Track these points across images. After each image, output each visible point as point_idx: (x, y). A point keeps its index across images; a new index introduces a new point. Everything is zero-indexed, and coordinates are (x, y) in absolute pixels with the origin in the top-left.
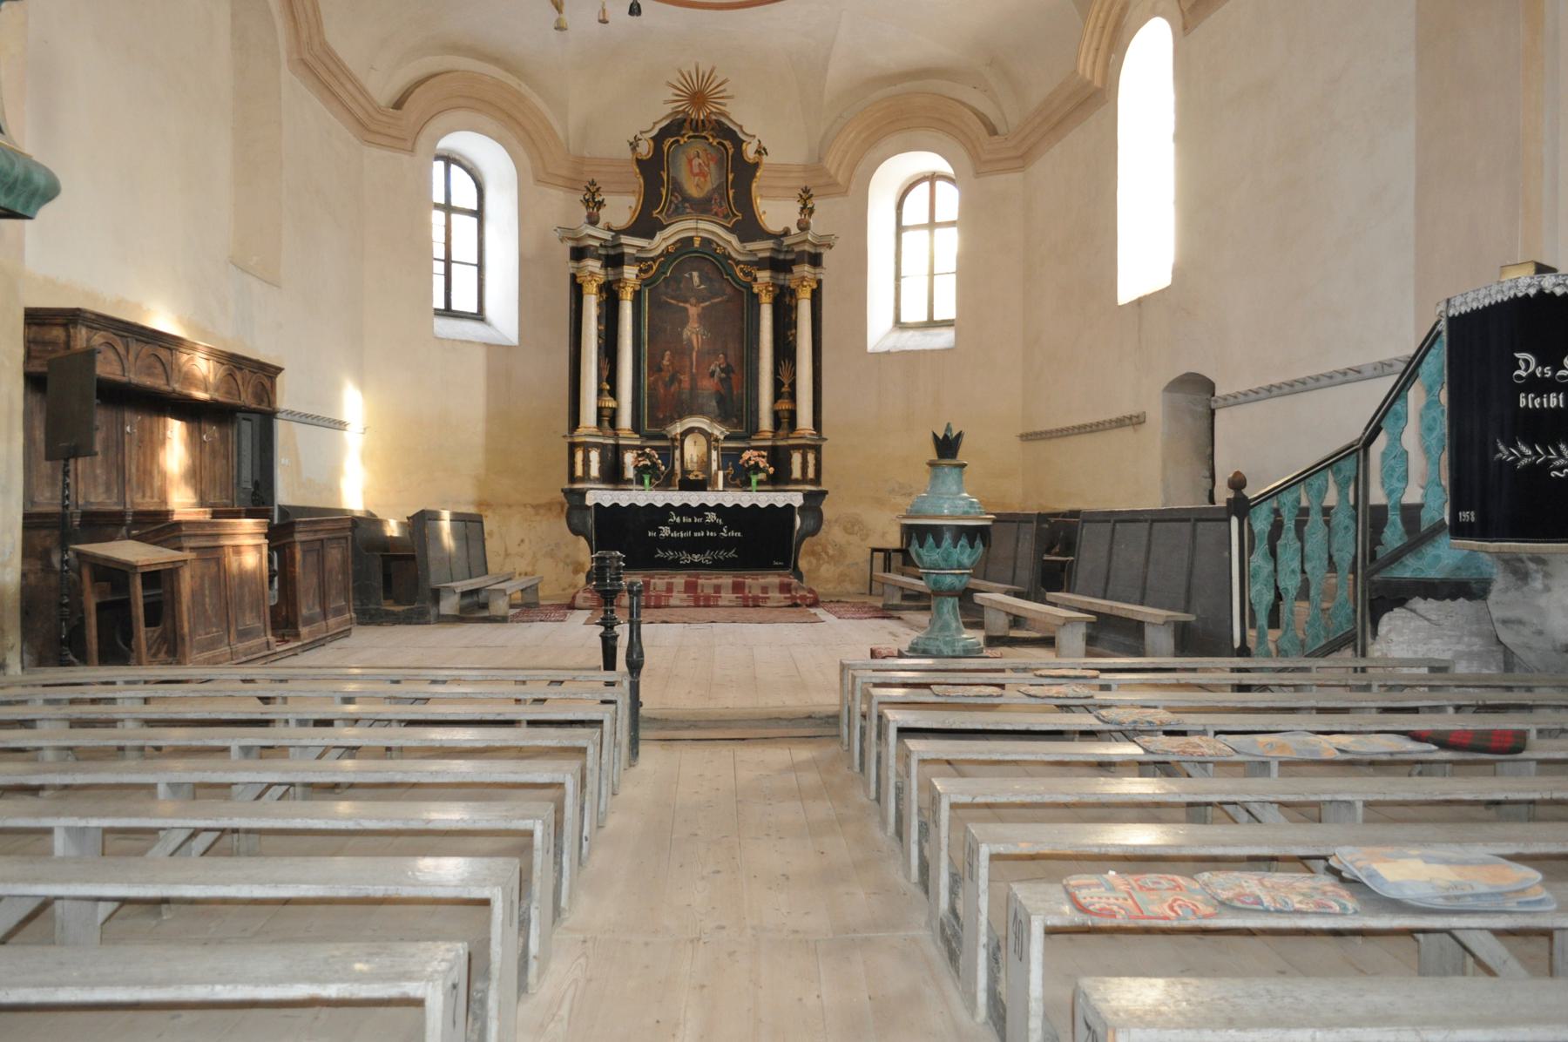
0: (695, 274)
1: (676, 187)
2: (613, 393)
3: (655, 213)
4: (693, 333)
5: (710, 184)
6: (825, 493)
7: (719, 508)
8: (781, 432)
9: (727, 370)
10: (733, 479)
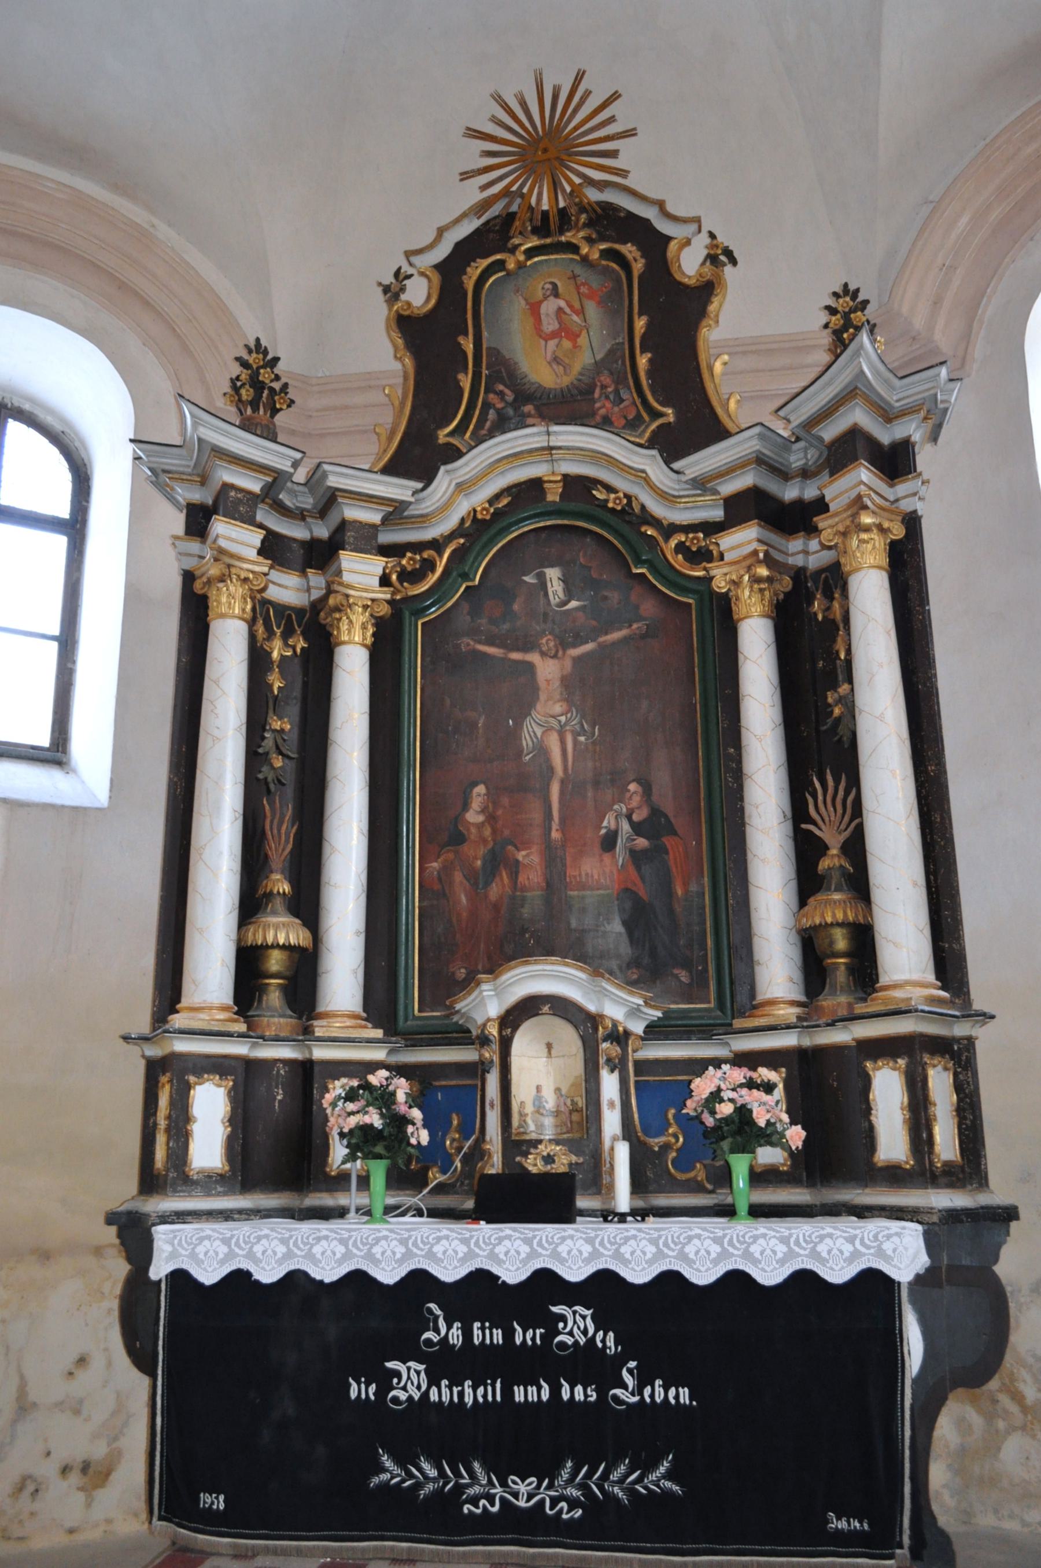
0: (553, 574)
1: (501, 371)
2: (307, 906)
3: (443, 435)
4: (550, 728)
6: (1008, 1215)
7: (603, 1289)
8: (836, 1001)
9: (654, 826)
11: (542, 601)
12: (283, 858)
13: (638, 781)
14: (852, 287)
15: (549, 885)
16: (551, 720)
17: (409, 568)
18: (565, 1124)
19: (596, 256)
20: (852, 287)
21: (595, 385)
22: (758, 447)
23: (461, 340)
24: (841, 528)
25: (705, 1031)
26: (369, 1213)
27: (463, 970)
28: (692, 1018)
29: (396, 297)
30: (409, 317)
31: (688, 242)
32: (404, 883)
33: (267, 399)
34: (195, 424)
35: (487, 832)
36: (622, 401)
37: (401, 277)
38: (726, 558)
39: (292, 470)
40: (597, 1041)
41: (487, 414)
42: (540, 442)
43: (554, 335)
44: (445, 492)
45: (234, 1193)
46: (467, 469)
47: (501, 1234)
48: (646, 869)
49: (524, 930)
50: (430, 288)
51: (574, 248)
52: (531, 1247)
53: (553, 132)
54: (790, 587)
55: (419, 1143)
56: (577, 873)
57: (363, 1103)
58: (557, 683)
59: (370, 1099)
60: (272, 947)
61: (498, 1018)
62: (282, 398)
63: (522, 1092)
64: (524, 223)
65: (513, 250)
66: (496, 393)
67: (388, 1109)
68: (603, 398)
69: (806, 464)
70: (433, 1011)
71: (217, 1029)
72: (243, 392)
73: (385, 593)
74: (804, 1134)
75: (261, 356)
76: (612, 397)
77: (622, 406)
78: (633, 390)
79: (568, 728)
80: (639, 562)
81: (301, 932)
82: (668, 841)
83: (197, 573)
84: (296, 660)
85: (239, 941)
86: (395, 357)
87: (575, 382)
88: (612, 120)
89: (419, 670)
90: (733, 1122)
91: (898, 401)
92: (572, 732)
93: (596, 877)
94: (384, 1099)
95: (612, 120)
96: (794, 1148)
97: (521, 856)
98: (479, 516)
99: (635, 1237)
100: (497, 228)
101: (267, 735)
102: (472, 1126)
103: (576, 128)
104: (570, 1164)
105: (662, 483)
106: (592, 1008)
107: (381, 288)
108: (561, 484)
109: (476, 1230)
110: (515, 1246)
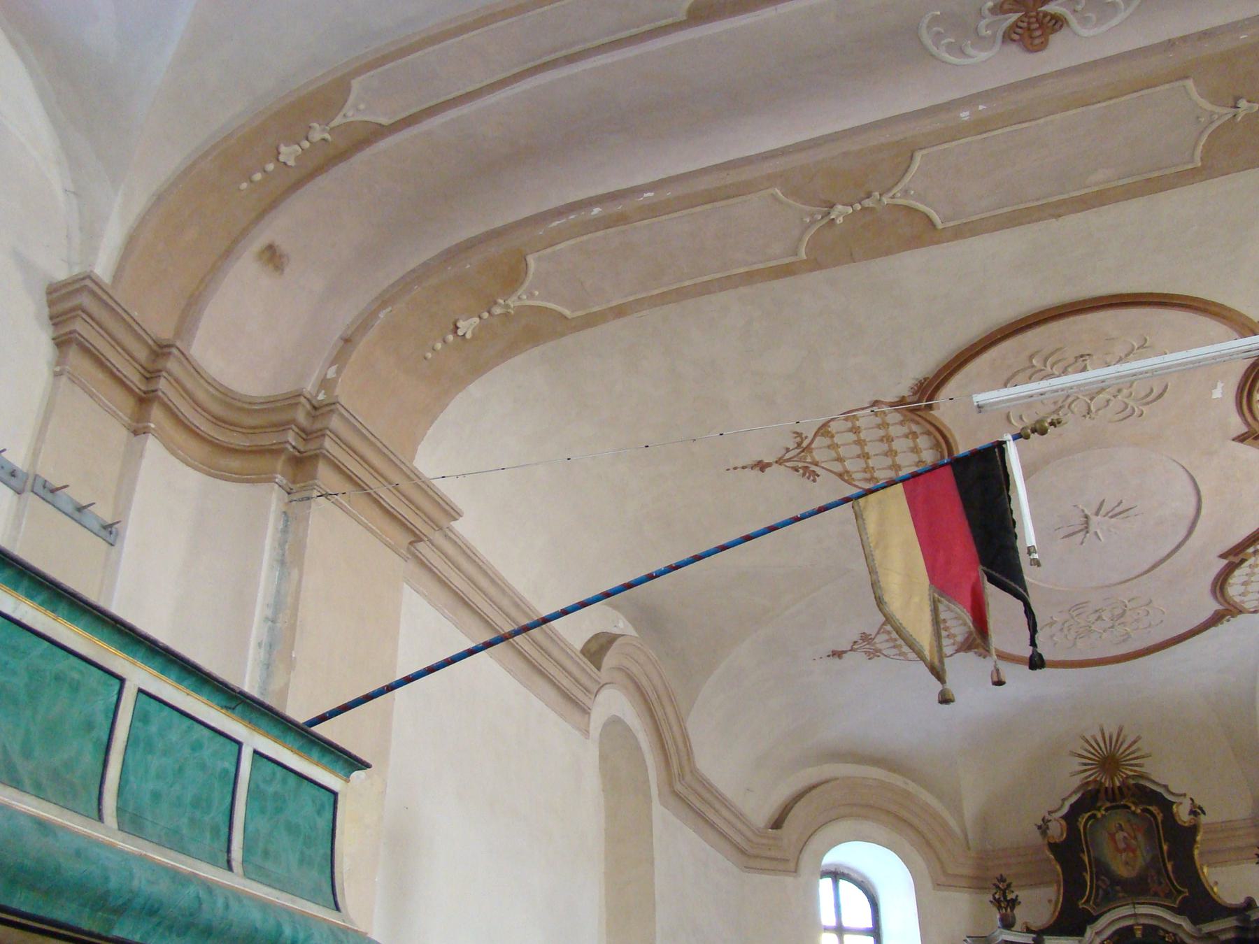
1: (1101, 869)
3: (1081, 904)
5: (1142, 858)
43: (1125, 850)
95: (1139, 749)
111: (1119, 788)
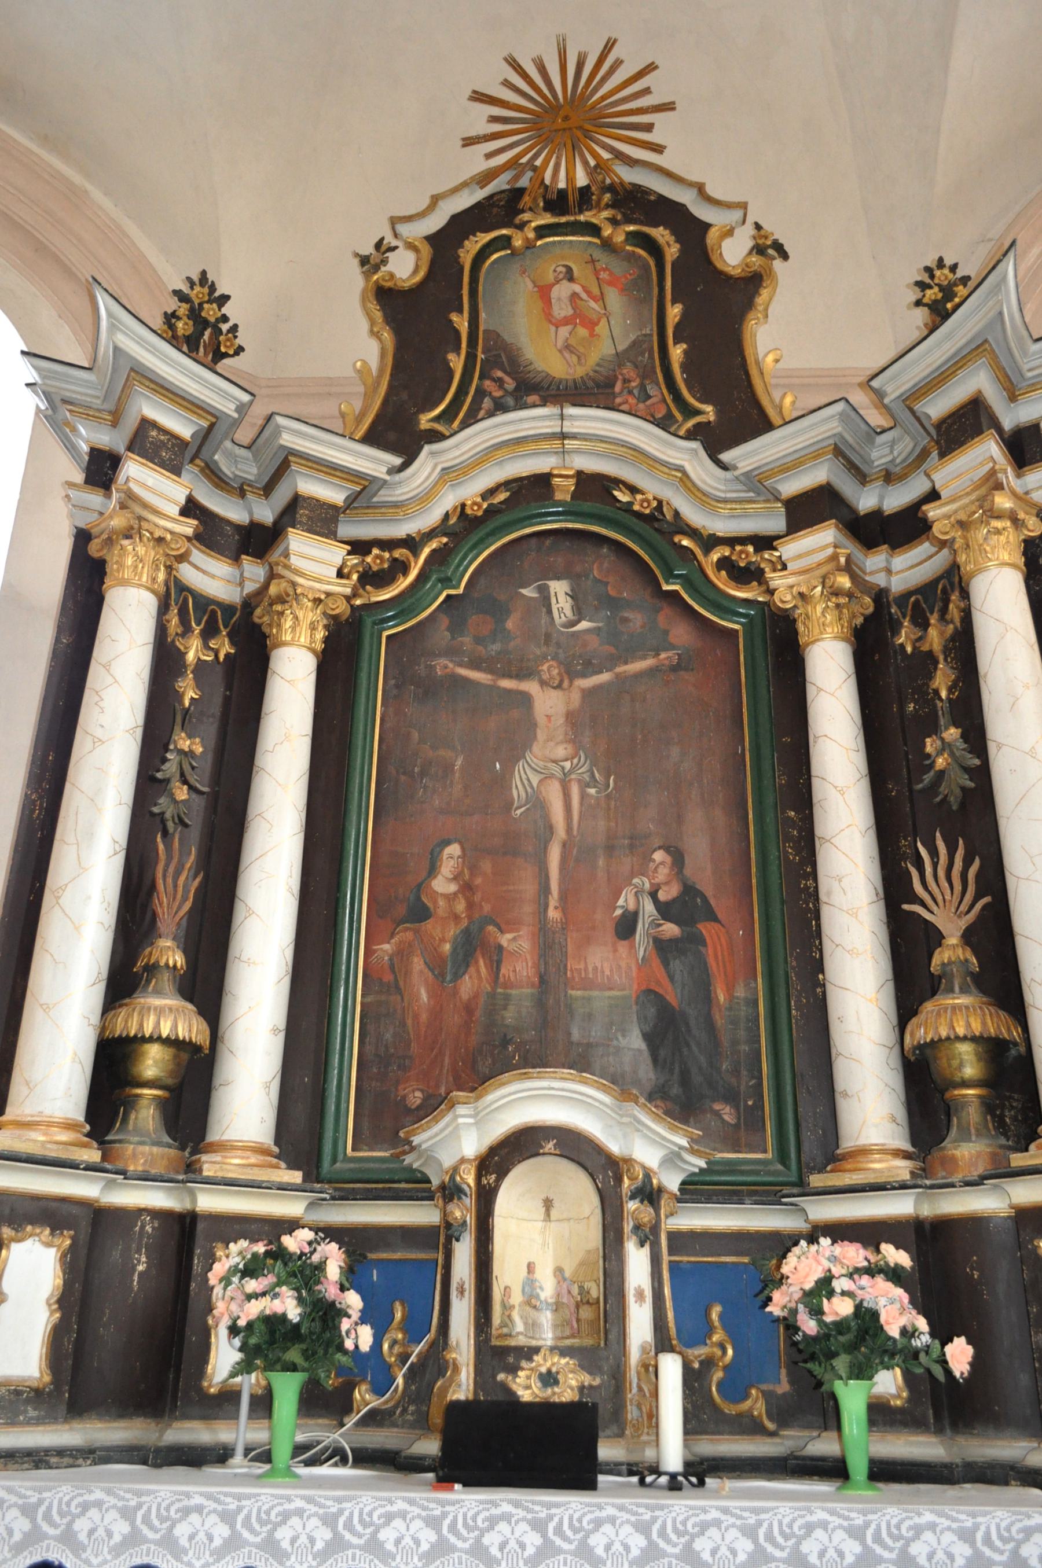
3: (425, 421)
4: (551, 775)
9: (687, 908)
10: (736, 1386)
11: (544, 619)
12: (177, 918)
13: (667, 849)
14: (948, 262)
15: (543, 980)
16: (550, 765)
17: (375, 568)
18: (569, 1323)
19: (619, 238)
20: (948, 262)
21: (616, 378)
22: (840, 429)
23: (454, 317)
24: (962, 516)
25: (768, 1194)
26: (266, 1457)
27: (418, 1094)
28: (742, 1173)
29: (376, 268)
30: (390, 289)
31: (730, 232)
32: (344, 968)
33: (210, 338)
34: (113, 328)
35: (460, 906)
36: (649, 397)
37: (383, 248)
38: (789, 568)
39: (236, 415)
40: (621, 1198)
41: (482, 402)
42: (552, 426)
43: (566, 321)
44: (427, 478)
45: (54, 1420)
46: (457, 453)
47: (495, 1511)
48: (676, 965)
49: (505, 1042)
50: (418, 259)
51: (594, 230)
52: (544, 1536)
53: (577, 100)
54: (871, 609)
55: (357, 1347)
56: (582, 966)
57: (271, 1279)
58: (561, 721)
59: (283, 1274)
60: (151, 1040)
61: (475, 1160)
62: (228, 340)
63: (507, 1273)
64: (535, 200)
65: (521, 227)
66: (494, 380)
67: (310, 1290)
68: (626, 391)
69: (893, 461)
70: (372, 1150)
71: (54, 1154)
72: (180, 325)
73: (344, 585)
74: (970, 1350)
75: (206, 290)
76: (636, 392)
77: (648, 403)
78: (663, 387)
79: (573, 776)
80: (670, 576)
81: (195, 1021)
82: (705, 928)
83: (94, 531)
84: (219, 669)
85: (103, 1029)
86: (372, 331)
87: (592, 374)
88: (647, 91)
89: (380, 693)
90: (849, 1329)
91: (1030, 370)
92: (579, 781)
93: (607, 973)
94: (304, 1274)
95: (647, 91)
96: (958, 1375)
97: (505, 939)
98: (469, 511)
99: (717, 1523)
100: (502, 203)
101: (169, 756)
102: (428, 1321)
103: (603, 98)
104: (582, 1388)
105: (705, 483)
106: (615, 1148)
107: (356, 262)
108: (573, 481)
109: (453, 1503)
110: (517, 1534)
111: (585, 191)
